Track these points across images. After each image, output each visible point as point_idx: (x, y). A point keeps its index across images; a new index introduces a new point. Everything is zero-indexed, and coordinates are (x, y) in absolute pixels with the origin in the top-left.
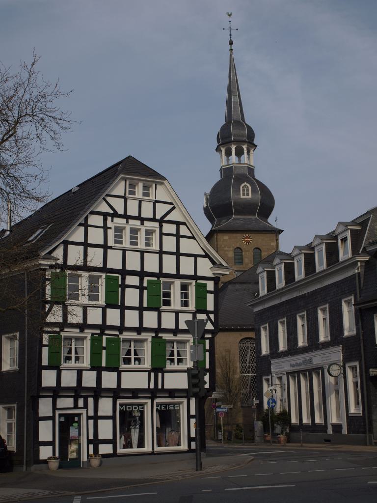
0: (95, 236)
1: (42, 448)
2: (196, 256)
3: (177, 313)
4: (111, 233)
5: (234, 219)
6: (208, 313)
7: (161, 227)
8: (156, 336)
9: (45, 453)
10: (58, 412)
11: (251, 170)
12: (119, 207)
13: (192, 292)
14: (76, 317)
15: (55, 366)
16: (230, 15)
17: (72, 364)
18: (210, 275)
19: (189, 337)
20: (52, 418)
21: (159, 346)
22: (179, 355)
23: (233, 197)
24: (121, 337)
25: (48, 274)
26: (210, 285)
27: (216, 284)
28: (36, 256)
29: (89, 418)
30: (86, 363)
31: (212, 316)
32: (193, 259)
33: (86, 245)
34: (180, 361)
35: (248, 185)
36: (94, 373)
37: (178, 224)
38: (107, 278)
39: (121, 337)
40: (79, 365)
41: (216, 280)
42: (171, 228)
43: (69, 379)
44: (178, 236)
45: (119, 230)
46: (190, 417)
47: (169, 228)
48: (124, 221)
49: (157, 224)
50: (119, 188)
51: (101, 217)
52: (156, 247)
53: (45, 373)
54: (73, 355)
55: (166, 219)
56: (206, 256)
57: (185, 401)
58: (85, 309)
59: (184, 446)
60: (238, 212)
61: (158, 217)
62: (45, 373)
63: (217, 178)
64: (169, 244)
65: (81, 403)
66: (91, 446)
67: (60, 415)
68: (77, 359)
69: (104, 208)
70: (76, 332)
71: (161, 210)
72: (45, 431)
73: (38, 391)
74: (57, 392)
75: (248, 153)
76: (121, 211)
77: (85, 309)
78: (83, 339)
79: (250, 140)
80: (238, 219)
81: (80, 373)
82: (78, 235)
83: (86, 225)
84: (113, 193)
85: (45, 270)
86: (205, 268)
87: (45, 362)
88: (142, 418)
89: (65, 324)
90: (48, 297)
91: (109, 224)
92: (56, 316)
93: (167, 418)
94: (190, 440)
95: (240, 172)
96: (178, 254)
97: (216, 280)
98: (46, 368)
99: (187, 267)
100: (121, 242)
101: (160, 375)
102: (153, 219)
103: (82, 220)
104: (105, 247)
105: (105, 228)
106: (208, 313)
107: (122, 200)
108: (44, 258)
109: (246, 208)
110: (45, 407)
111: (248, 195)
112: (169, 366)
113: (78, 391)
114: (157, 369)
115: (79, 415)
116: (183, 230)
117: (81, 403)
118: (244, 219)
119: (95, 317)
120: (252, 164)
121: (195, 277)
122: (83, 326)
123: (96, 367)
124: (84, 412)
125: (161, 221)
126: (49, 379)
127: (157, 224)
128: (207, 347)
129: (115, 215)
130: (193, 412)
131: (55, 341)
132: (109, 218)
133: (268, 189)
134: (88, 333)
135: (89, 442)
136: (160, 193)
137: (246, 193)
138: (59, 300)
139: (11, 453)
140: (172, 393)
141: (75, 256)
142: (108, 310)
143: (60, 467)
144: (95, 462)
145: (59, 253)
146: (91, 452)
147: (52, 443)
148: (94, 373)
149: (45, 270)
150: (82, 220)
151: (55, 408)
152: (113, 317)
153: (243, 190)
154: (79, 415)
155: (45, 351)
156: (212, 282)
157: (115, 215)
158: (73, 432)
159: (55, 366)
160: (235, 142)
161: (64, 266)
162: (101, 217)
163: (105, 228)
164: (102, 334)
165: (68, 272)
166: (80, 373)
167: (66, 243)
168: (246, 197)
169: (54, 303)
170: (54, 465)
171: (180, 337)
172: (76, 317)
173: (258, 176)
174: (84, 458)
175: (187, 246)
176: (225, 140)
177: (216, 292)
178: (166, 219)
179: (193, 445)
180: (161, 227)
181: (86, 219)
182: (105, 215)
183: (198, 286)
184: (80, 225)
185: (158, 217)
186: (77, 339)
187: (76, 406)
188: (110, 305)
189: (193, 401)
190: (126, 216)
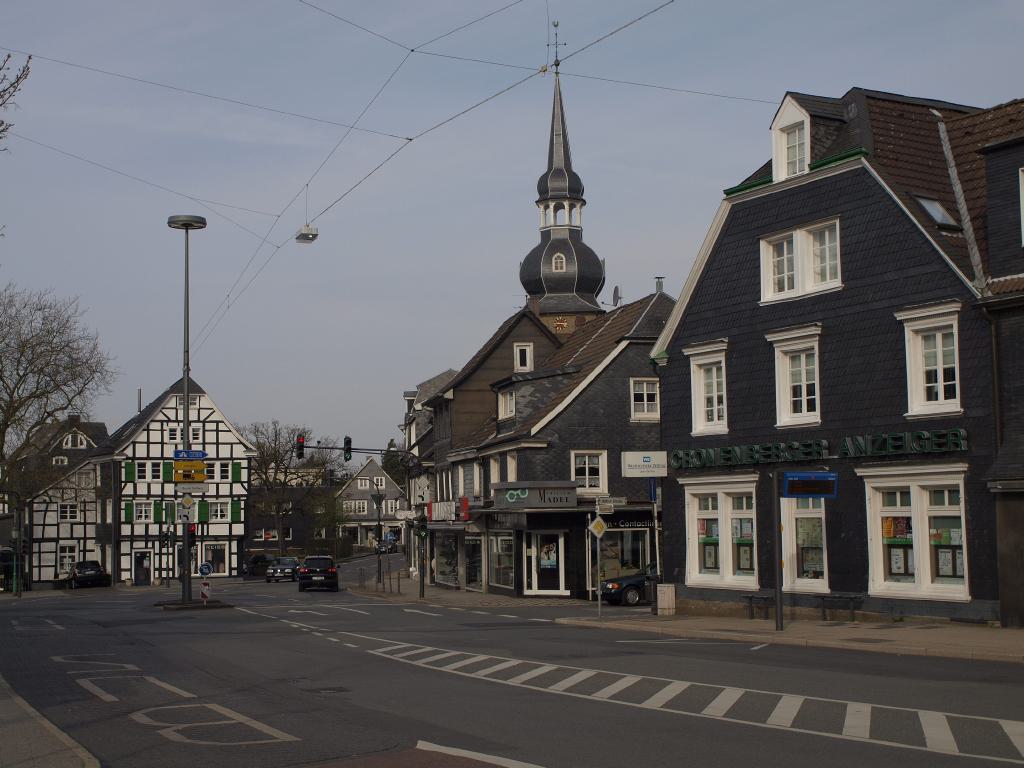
0: (155, 436)
1: (123, 573)
2: (232, 444)
3: (218, 484)
4: (166, 434)
5: (547, 298)
6: (242, 483)
7: (204, 426)
8: (203, 500)
9: (125, 576)
10: (133, 551)
11: (576, 233)
12: (171, 414)
13: (230, 468)
14: (142, 489)
15: (129, 521)
16: (556, 26)
17: (143, 520)
18: (243, 456)
19: (229, 500)
20: (130, 554)
21: (204, 507)
22: (221, 511)
23: (544, 270)
24: (176, 502)
25: (123, 464)
26: (244, 463)
27: (249, 463)
28: (112, 453)
29: (155, 554)
30: (152, 520)
31: (246, 485)
32: (229, 446)
33: (148, 443)
34: (222, 516)
35: (562, 256)
36: (157, 526)
37: (217, 422)
38: (164, 464)
39: (176, 502)
40: (148, 521)
41: (249, 459)
42: (213, 426)
43: (139, 530)
44: (217, 431)
45: (173, 432)
46: (231, 554)
47: (209, 426)
48: (176, 424)
49: (201, 425)
50: (172, 403)
51: (159, 424)
52: (201, 440)
53: (123, 526)
54: (143, 514)
55: (210, 419)
56: (241, 443)
57: (227, 543)
58: (149, 485)
59: (227, 574)
60: (551, 290)
61: (202, 419)
62: (123, 526)
63: (537, 240)
64: (211, 437)
65: (150, 545)
66: (157, 573)
67: (136, 553)
68: (146, 517)
69: (161, 417)
70: (144, 500)
71: (204, 414)
72: (125, 562)
73: (118, 539)
74: (132, 538)
75: (570, 210)
76: (173, 418)
77: (149, 485)
78: (150, 504)
79: (575, 194)
80: (552, 298)
81: (147, 526)
82: (143, 437)
83: (148, 430)
84: (168, 406)
85: (120, 462)
86: (239, 451)
87: (123, 519)
88: (196, 554)
89: (135, 495)
90: (123, 479)
91: (165, 427)
92: (128, 490)
93: (218, 557)
94: (231, 569)
95: (558, 237)
96: (217, 444)
97: (249, 459)
98: (124, 523)
99: (225, 452)
100: (175, 439)
101: (205, 526)
102: (198, 421)
103: (145, 426)
104: (162, 443)
105: (162, 430)
106: (242, 483)
107: (174, 411)
108: (117, 455)
109: (560, 284)
110: (125, 547)
111: (562, 268)
112: (211, 522)
113: (147, 538)
114: (204, 522)
115: (150, 552)
116: (222, 427)
117: (150, 545)
118: (559, 297)
119: (156, 489)
120: (578, 224)
121: (232, 458)
122: (149, 496)
123: (160, 523)
124: (152, 551)
125: (204, 422)
126: (126, 530)
127: (201, 425)
128: (243, 506)
129: (169, 421)
130: (234, 549)
131: (129, 507)
132: (165, 424)
133: (596, 256)
134: (152, 501)
135: (155, 569)
136: (205, 402)
137: (560, 266)
138: (130, 479)
139: (108, 576)
140: (216, 538)
141: (141, 451)
142: (166, 485)
143: (132, 585)
144: (157, 582)
145: (129, 452)
146: (157, 575)
147: (130, 570)
148: (157, 526)
149: (120, 462)
150: (145, 426)
151: (132, 548)
152: (170, 489)
153: (556, 263)
154: (150, 552)
155: (123, 513)
156: (246, 461)
157: (169, 421)
158: (146, 563)
159: (129, 521)
160: (553, 198)
161: (134, 458)
162: (159, 424)
163: (162, 430)
164: (162, 500)
165: (136, 462)
166: (147, 526)
167: (134, 443)
168: (559, 271)
169: (126, 482)
170: (128, 583)
171: (221, 500)
172: (142, 489)
173: (587, 240)
174: (152, 579)
175: (223, 437)
176: (545, 196)
177: (249, 468)
178: (210, 419)
179: (234, 573)
180: (204, 426)
181: (148, 426)
182: (162, 422)
183: (233, 464)
184: (144, 430)
185: (202, 419)
186: (146, 504)
187: (146, 547)
188: (167, 480)
189: (234, 544)
190: (177, 421)
